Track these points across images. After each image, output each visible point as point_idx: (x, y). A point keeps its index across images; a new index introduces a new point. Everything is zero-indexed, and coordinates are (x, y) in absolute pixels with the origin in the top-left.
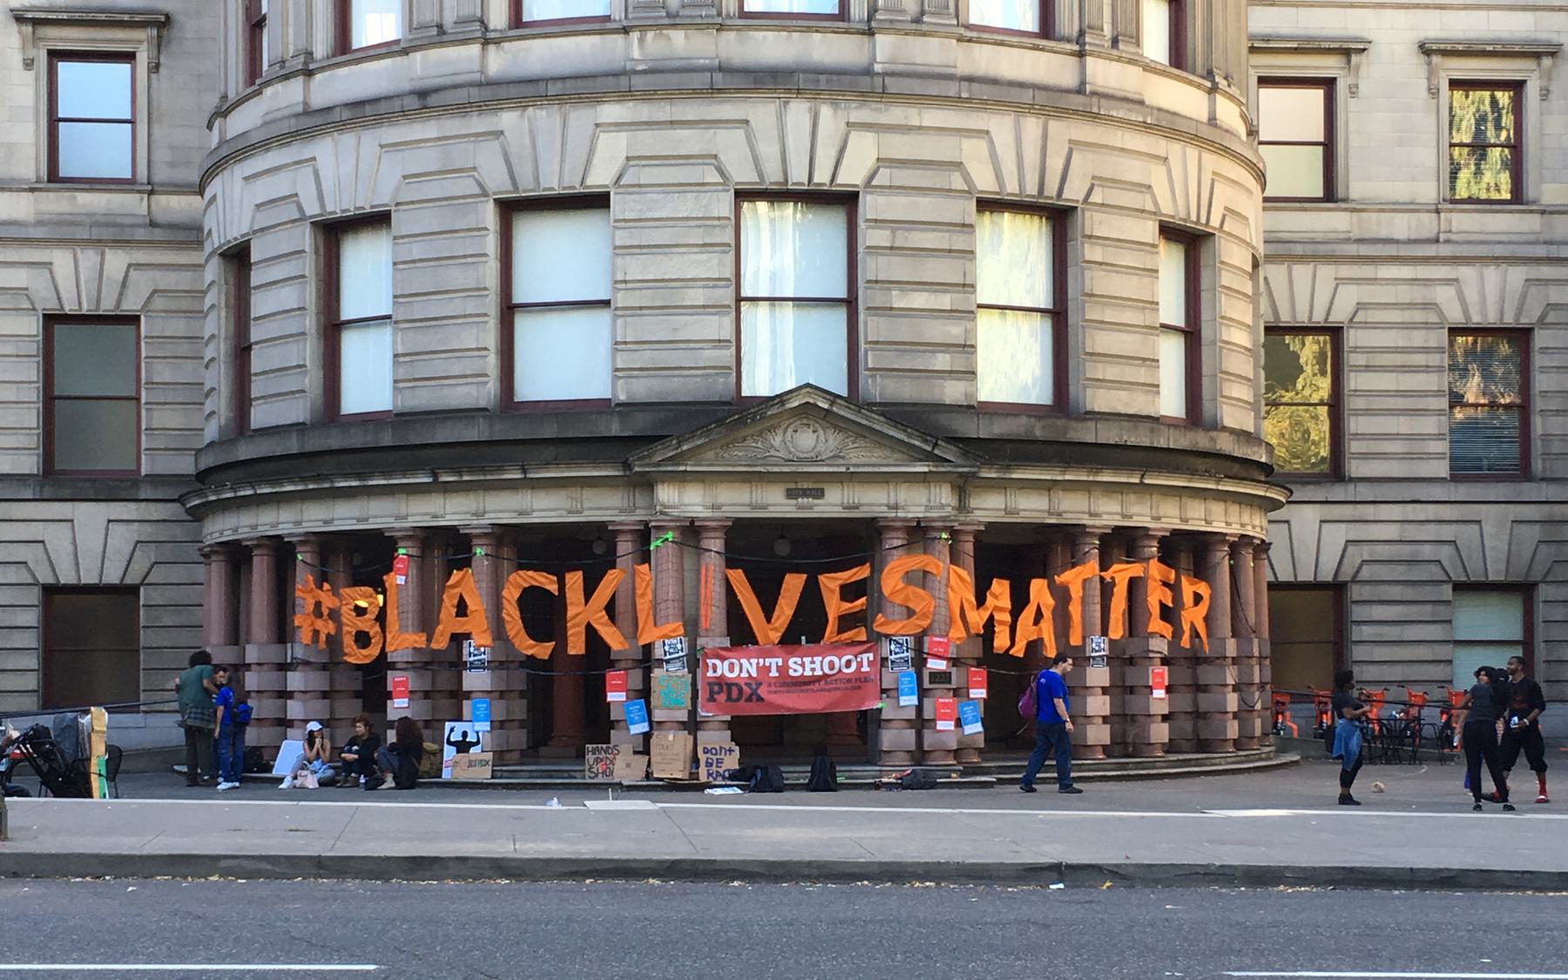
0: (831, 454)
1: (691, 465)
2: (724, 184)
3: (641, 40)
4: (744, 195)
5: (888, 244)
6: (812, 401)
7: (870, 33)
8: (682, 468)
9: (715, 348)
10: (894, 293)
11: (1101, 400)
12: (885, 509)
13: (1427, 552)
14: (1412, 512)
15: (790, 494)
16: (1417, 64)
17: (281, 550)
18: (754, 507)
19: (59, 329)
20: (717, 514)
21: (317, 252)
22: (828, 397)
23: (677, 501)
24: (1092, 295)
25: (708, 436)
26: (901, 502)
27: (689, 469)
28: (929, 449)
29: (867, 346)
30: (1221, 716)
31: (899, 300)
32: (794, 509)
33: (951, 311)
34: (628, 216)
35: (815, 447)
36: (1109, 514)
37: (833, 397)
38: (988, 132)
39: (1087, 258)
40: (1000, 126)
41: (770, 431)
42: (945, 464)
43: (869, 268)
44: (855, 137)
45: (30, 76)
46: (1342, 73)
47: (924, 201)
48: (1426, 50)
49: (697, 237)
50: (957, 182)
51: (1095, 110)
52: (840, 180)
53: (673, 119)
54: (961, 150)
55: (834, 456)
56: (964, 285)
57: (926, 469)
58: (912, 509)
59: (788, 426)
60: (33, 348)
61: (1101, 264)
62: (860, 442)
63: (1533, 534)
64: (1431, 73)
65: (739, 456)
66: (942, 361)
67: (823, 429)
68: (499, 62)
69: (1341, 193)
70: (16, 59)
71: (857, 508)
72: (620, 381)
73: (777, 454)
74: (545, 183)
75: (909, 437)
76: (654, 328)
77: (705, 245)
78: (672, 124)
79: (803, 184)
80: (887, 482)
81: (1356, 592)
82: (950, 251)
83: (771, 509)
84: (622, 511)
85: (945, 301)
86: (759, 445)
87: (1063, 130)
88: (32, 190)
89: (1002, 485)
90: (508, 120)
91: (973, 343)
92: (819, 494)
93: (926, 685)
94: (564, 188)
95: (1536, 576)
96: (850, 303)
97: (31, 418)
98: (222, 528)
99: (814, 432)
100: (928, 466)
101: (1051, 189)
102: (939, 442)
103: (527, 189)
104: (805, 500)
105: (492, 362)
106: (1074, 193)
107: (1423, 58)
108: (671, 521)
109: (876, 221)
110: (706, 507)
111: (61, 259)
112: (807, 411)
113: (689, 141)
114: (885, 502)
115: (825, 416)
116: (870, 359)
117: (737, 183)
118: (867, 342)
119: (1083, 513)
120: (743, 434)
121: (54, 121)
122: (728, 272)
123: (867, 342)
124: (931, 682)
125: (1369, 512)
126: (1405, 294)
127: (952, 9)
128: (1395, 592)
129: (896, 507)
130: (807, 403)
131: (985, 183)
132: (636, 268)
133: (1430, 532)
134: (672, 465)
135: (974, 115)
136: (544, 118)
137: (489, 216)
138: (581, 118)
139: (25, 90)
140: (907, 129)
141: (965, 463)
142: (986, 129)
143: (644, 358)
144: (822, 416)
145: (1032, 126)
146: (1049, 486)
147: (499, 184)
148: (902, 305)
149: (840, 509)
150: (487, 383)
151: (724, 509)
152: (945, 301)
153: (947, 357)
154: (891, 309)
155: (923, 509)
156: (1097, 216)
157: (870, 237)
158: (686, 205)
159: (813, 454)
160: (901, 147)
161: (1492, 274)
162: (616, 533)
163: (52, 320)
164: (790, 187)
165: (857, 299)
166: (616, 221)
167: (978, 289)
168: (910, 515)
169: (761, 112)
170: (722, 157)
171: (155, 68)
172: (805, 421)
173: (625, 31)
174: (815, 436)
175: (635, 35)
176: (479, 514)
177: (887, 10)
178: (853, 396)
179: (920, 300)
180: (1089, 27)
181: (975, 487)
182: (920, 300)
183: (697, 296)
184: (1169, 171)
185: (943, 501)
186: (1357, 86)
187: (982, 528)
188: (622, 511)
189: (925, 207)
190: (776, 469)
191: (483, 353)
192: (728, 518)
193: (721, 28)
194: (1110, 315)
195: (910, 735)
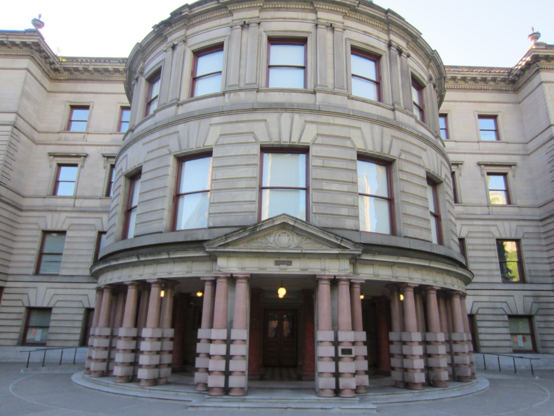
0: (296, 246)
1: (231, 248)
2: (256, 142)
3: (229, 96)
4: (265, 149)
5: (321, 165)
6: (286, 221)
7: (314, 93)
9: (249, 204)
10: (324, 183)
11: (411, 232)
12: (320, 271)
13: (498, 305)
14: (492, 293)
15: (277, 263)
16: (477, 169)
18: (260, 269)
20: (244, 272)
21: (126, 185)
22: (293, 219)
23: (226, 265)
24: (404, 192)
26: (327, 268)
27: (230, 250)
28: (338, 242)
29: (312, 204)
30: (464, 366)
31: (326, 186)
32: (278, 270)
33: (348, 192)
34: (219, 155)
35: (288, 243)
36: (417, 278)
37: (296, 220)
38: (360, 128)
39: (401, 178)
40: (366, 126)
41: (268, 235)
42: (347, 250)
43: (314, 174)
44: (308, 126)
45: (105, 170)
46: (457, 170)
47: (336, 150)
48: (479, 164)
49: (244, 161)
50: (349, 144)
51: (400, 126)
52: (302, 141)
53: (238, 120)
54: (350, 133)
55: (296, 247)
56: (353, 182)
57: (337, 252)
58: (332, 271)
59: (277, 233)
60: (94, 240)
61: (406, 181)
62: (308, 241)
63: (531, 300)
64: (481, 170)
65: (254, 246)
66: (344, 211)
67: (293, 236)
68: (181, 110)
69: (459, 201)
71: (306, 270)
72: (210, 218)
73: (271, 245)
74: (190, 147)
75: (330, 237)
77: (247, 165)
78: (237, 122)
79: (287, 142)
80: (321, 259)
82: (347, 169)
83: (268, 270)
84: (207, 272)
85: (345, 188)
86: (264, 241)
87: (389, 132)
88: (100, 199)
90: (181, 127)
91: (357, 205)
92: (290, 263)
93: (340, 354)
94: (197, 148)
95: (533, 313)
96: (307, 189)
99: (288, 236)
100: (339, 250)
101: (386, 151)
104: (283, 266)
105: (167, 215)
106: (394, 154)
107: (479, 167)
108: (222, 274)
109: (316, 156)
110: (239, 269)
112: (284, 226)
115: (293, 229)
116: (314, 209)
117: (261, 142)
118: (313, 203)
119: (407, 277)
120: (256, 237)
122: (256, 174)
123: (313, 203)
125: (479, 292)
126: (481, 229)
127: (345, 87)
128: (491, 318)
130: (284, 223)
131: (360, 146)
132: (222, 174)
134: (223, 248)
135: (354, 121)
136: (193, 125)
137: (172, 161)
138: (205, 123)
140: (329, 124)
141: (355, 249)
142: (360, 127)
144: (292, 229)
145: (377, 128)
147: (175, 149)
148: (327, 188)
149: (299, 270)
150: (163, 222)
152: (345, 188)
153: (347, 210)
154: (323, 190)
155: (337, 271)
156: (404, 164)
157: (314, 162)
158: (241, 150)
159: (287, 246)
160: (325, 130)
161: (506, 224)
162: (205, 281)
164: (282, 143)
165: (309, 187)
166: (214, 158)
167: (359, 184)
168: (331, 274)
169: (272, 117)
170: (256, 133)
172: (284, 231)
174: (289, 237)
175: (227, 95)
176: (154, 274)
177: (320, 85)
178: (307, 222)
179: (335, 187)
180: (396, 102)
181: (360, 264)
182: (335, 187)
183: (243, 184)
184: (428, 155)
185: (346, 267)
186: (461, 173)
188: (207, 272)
190: (270, 251)
191: (163, 211)
192: (247, 274)
193: (258, 91)
194: (411, 200)
195: (333, 380)
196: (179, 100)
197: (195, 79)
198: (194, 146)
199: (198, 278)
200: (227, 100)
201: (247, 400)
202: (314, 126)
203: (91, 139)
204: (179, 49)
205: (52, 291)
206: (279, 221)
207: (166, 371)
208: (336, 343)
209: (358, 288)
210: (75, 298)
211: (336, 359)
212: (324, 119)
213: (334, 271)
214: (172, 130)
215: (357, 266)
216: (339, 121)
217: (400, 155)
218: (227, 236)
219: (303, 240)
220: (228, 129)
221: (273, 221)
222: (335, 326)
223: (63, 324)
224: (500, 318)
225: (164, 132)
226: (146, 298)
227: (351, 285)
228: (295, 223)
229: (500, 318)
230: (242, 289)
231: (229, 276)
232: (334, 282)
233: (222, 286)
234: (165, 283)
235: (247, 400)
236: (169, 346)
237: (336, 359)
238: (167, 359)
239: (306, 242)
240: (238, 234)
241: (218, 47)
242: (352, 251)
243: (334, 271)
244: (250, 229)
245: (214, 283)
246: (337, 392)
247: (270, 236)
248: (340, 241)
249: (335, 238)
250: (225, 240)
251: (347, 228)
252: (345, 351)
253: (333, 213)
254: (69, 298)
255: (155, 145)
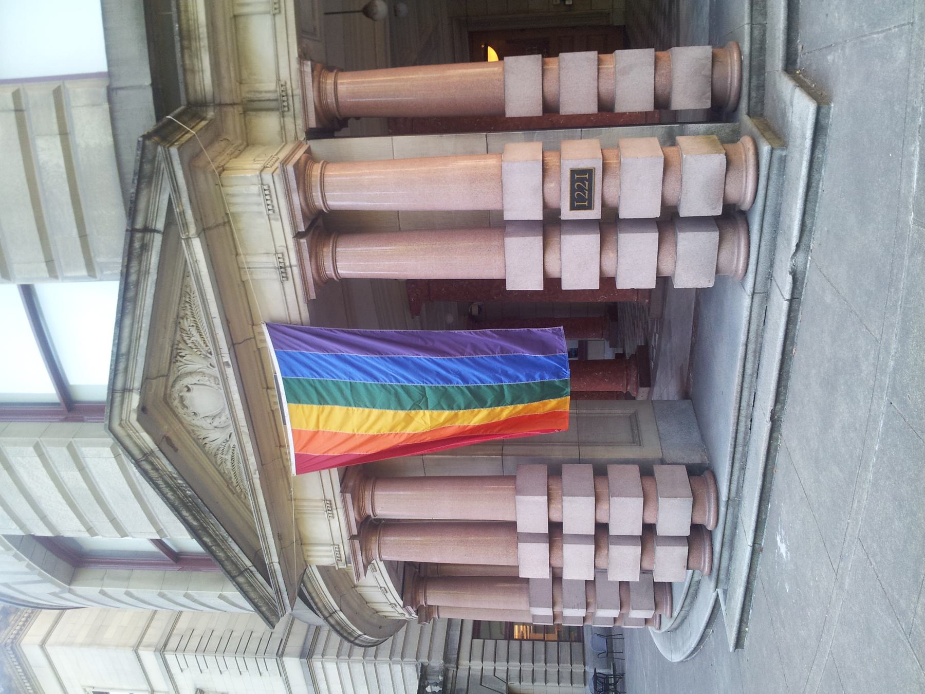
8: (277, 567)
12: (289, 285)
25: (224, 540)
26: (273, 261)
27: (275, 559)
28: (158, 239)
42: (177, 210)
58: (280, 242)
75: (147, 272)
86: (229, 457)
93: (595, 214)
99: (189, 390)
100: (188, 239)
102: (139, 225)
114: (276, 286)
124: (590, 207)
129: (283, 270)
151: (330, 496)
172: (176, 403)
183: (72, 477)
187: (308, 68)
201: (733, 494)
206: (141, 438)
209: (335, 84)
213: (278, 233)
215: (251, 96)
218: (234, 573)
219: (188, 342)
221: (145, 455)
226: (459, 568)
228: (131, 391)
231: (357, 543)
235: (733, 494)
239: (193, 331)
240: (218, 545)
242: (176, 188)
243: (278, 233)
244: (195, 518)
247: (206, 441)
248: (148, 236)
249: (141, 255)
250: (246, 574)
251: (110, 139)
252: (581, 199)
253: (66, 198)
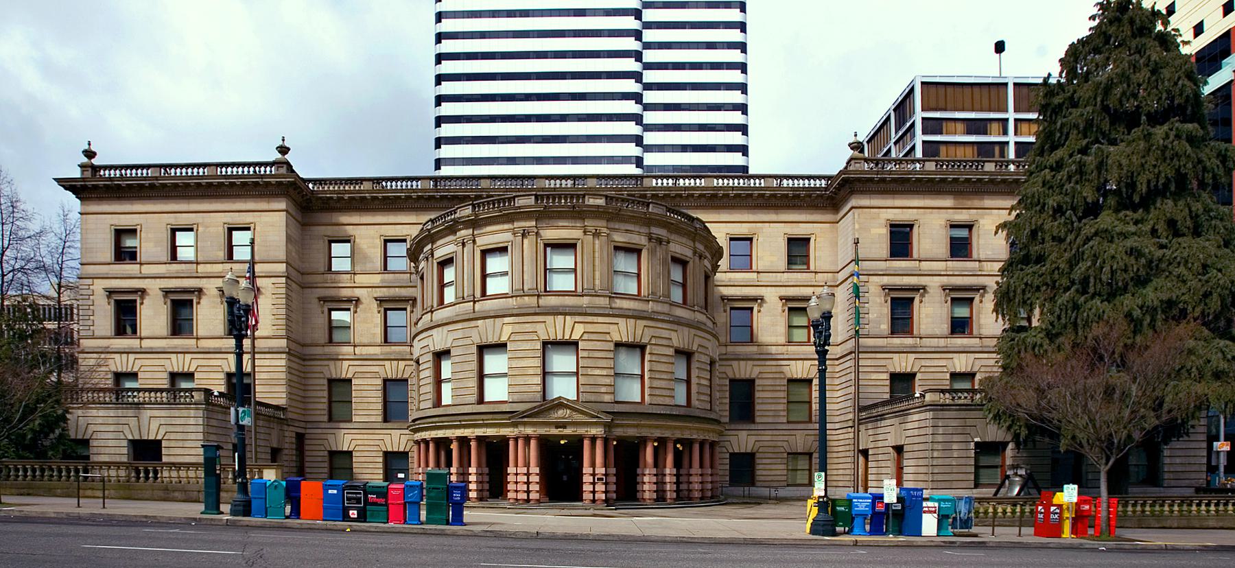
4: (545, 344)
13: (779, 444)
17: (426, 442)
19: (387, 383)
31: (590, 372)
69: (755, 340)
70: (376, 311)
76: (520, 380)
81: (758, 455)
89: (622, 426)
90: (480, 322)
97: (380, 406)
98: (419, 436)
101: (638, 340)
103: (484, 342)
105: (475, 390)
111: (387, 363)
113: (528, 327)
121: (386, 327)
125: (763, 432)
131: (617, 338)
132: (515, 364)
133: (781, 438)
139: (378, 319)
143: (517, 389)
145: (632, 321)
146: (637, 426)
147: (477, 340)
160: (590, 328)
163: (385, 381)
171: (412, 312)
173: (512, 297)
183: (531, 371)
189: (599, 345)
196: (474, 297)
197: (484, 276)
198: (492, 339)
199: (505, 436)
200: (512, 302)
202: (582, 325)
203: (360, 279)
204: (469, 247)
205: (350, 437)
207: (486, 494)
208: (594, 475)
210: (372, 443)
211: (594, 484)
212: (590, 319)
214: (473, 323)
216: (600, 319)
217: (651, 339)
220: (518, 328)
222: (593, 465)
223: (366, 465)
224: (780, 456)
225: (466, 324)
227: (606, 441)
229: (780, 456)
230: (533, 443)
232: (593, 439)
233: (520, 442)
234: (480, 439)
236: (486, 478)
237: (594, 484)
238: (487, 486)
241: (503, 250)
245: (516, 439)
246: (594, 501)
254: (366, 442)
255: (459, 334)
